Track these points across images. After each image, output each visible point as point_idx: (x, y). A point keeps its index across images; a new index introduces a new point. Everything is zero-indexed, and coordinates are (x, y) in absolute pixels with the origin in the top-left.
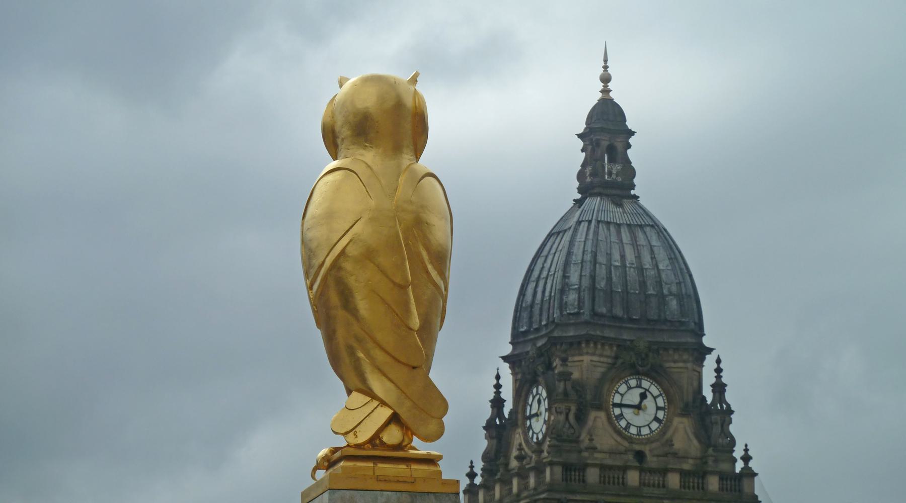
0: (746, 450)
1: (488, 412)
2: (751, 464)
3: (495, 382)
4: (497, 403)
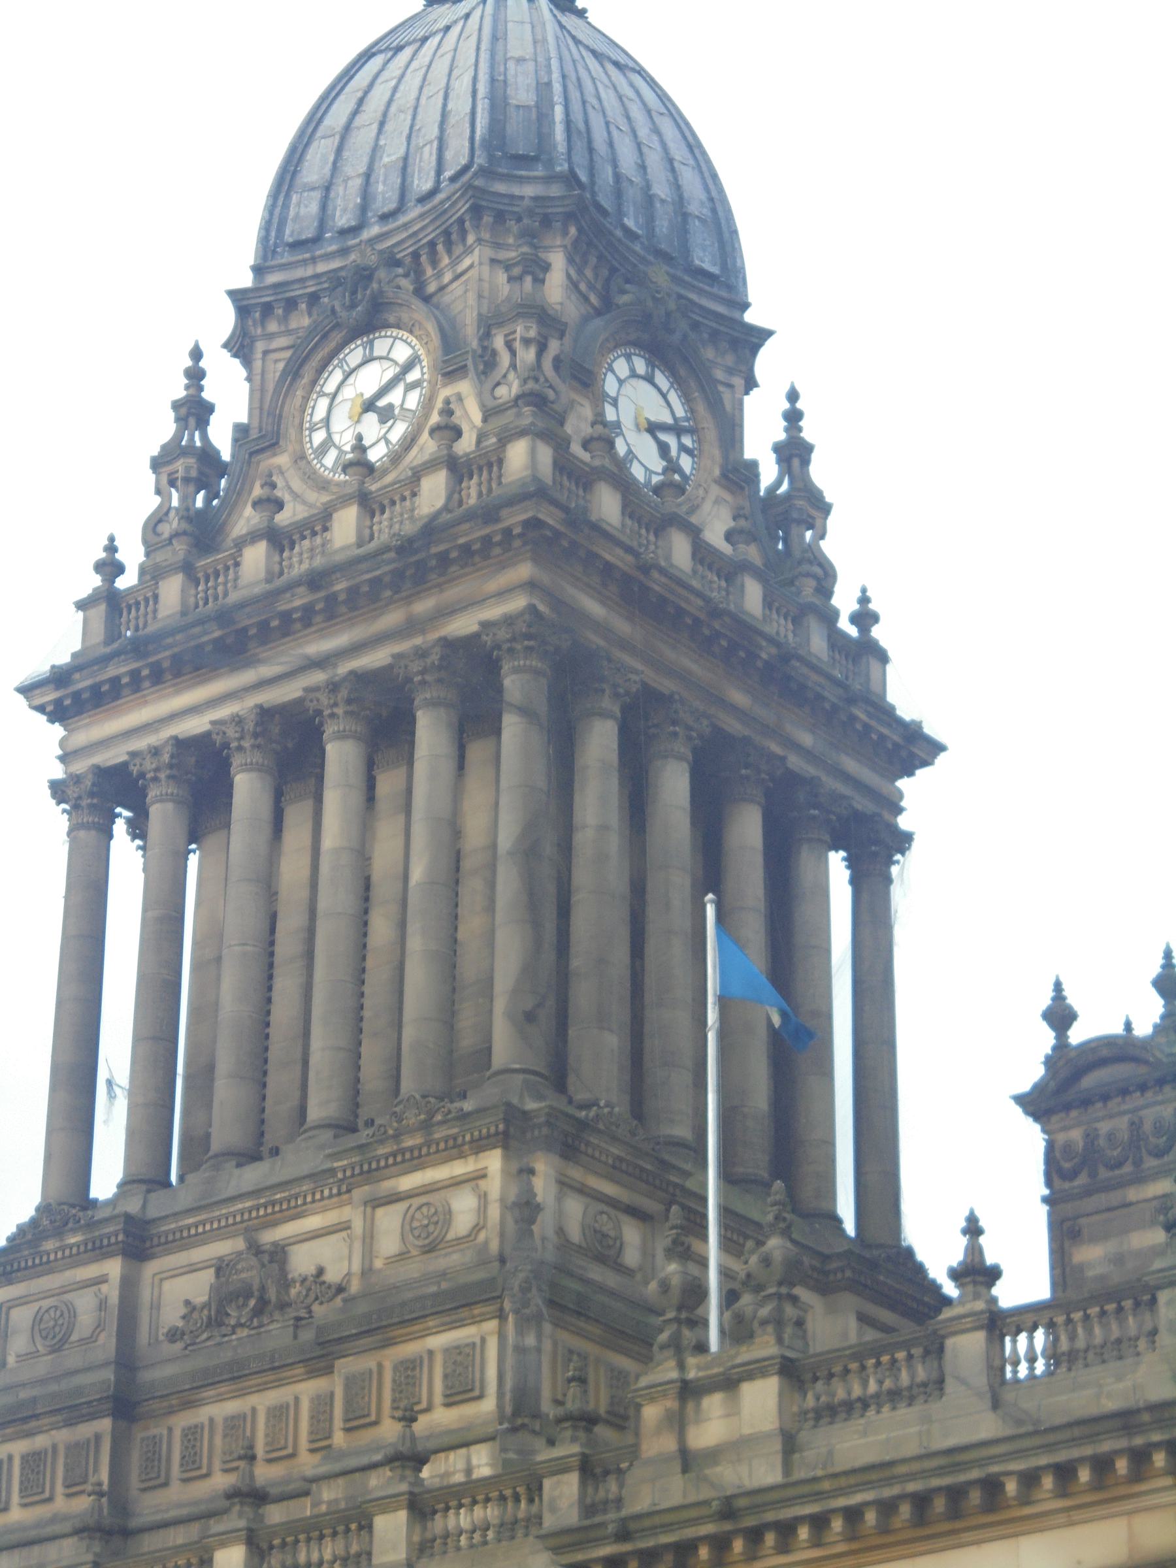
0: (864, 600)
1: (165, 428)
2: (876, 632)
3: (189, 363)
4: (194, 411)
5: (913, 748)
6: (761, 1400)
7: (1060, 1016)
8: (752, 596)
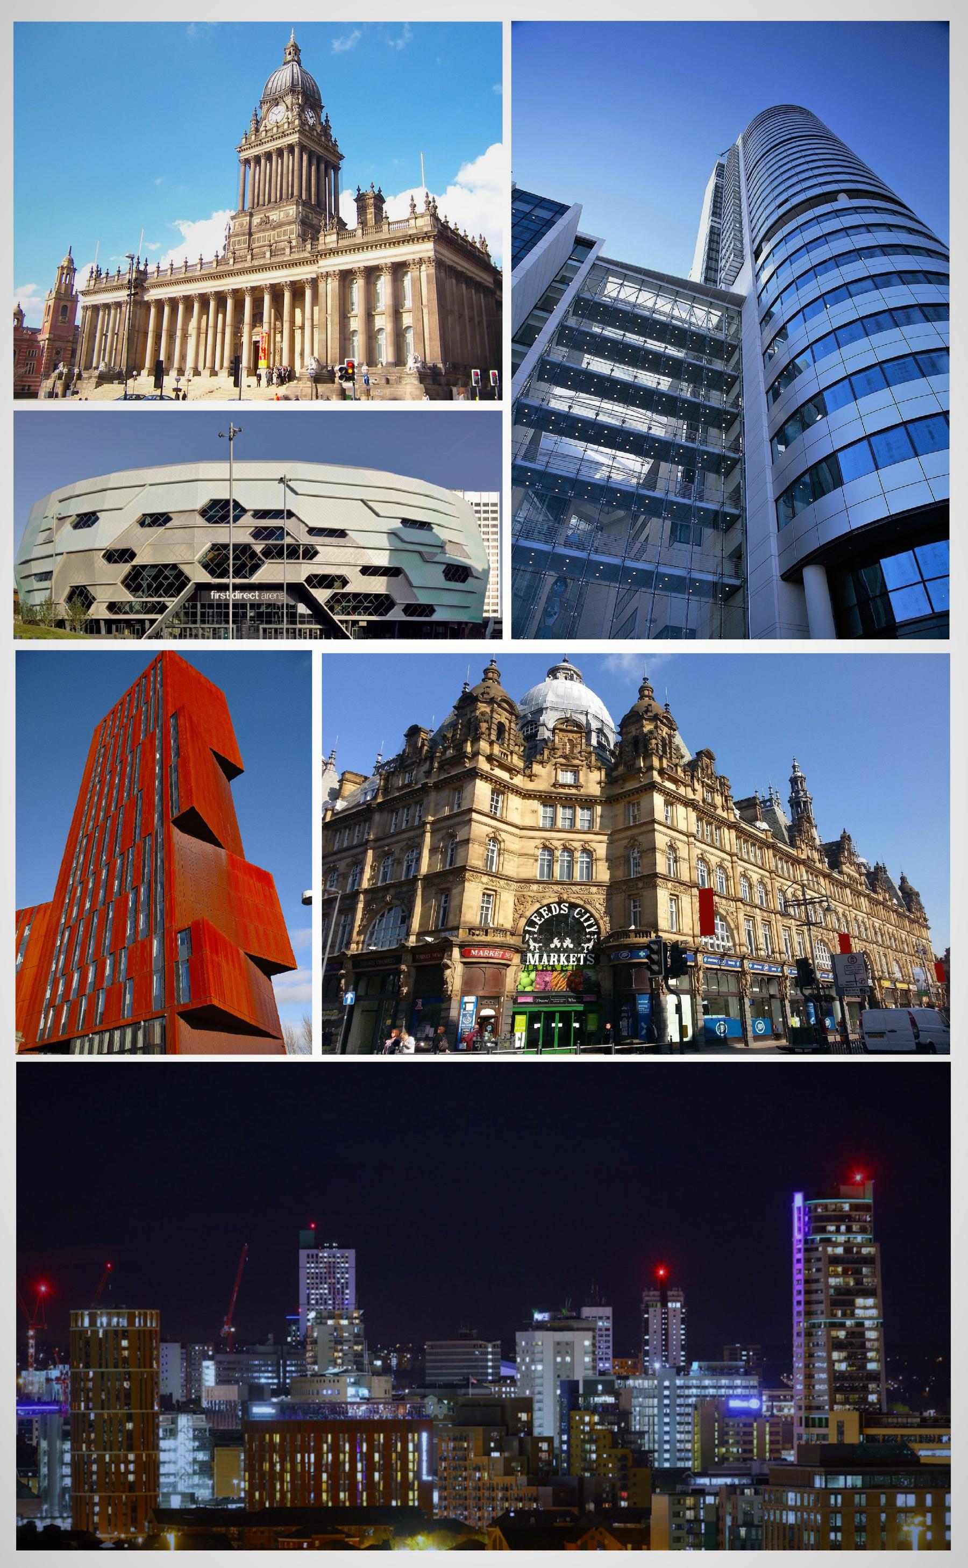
5: (341, 157)
6: (334, 237)
7: (359, 190)
8: (323, 138)
